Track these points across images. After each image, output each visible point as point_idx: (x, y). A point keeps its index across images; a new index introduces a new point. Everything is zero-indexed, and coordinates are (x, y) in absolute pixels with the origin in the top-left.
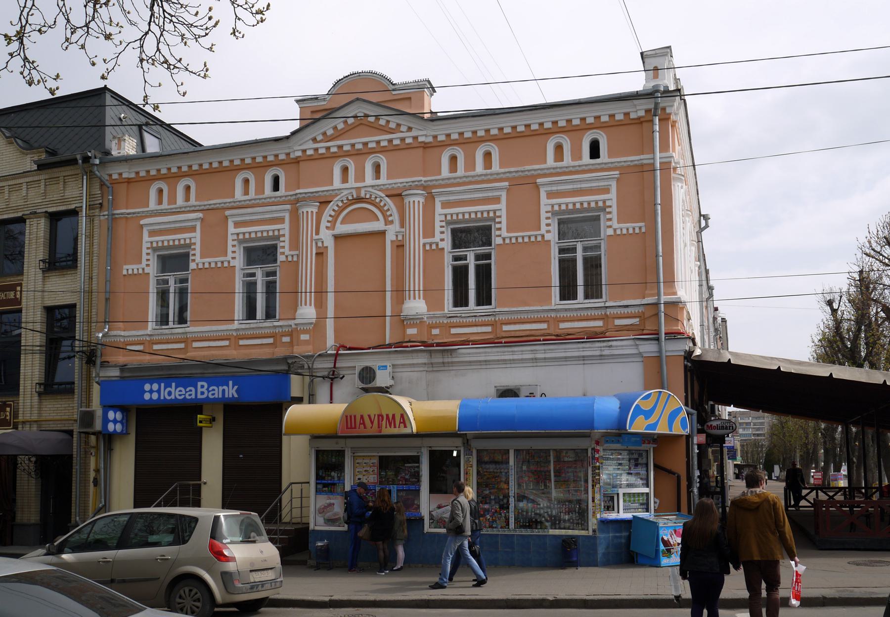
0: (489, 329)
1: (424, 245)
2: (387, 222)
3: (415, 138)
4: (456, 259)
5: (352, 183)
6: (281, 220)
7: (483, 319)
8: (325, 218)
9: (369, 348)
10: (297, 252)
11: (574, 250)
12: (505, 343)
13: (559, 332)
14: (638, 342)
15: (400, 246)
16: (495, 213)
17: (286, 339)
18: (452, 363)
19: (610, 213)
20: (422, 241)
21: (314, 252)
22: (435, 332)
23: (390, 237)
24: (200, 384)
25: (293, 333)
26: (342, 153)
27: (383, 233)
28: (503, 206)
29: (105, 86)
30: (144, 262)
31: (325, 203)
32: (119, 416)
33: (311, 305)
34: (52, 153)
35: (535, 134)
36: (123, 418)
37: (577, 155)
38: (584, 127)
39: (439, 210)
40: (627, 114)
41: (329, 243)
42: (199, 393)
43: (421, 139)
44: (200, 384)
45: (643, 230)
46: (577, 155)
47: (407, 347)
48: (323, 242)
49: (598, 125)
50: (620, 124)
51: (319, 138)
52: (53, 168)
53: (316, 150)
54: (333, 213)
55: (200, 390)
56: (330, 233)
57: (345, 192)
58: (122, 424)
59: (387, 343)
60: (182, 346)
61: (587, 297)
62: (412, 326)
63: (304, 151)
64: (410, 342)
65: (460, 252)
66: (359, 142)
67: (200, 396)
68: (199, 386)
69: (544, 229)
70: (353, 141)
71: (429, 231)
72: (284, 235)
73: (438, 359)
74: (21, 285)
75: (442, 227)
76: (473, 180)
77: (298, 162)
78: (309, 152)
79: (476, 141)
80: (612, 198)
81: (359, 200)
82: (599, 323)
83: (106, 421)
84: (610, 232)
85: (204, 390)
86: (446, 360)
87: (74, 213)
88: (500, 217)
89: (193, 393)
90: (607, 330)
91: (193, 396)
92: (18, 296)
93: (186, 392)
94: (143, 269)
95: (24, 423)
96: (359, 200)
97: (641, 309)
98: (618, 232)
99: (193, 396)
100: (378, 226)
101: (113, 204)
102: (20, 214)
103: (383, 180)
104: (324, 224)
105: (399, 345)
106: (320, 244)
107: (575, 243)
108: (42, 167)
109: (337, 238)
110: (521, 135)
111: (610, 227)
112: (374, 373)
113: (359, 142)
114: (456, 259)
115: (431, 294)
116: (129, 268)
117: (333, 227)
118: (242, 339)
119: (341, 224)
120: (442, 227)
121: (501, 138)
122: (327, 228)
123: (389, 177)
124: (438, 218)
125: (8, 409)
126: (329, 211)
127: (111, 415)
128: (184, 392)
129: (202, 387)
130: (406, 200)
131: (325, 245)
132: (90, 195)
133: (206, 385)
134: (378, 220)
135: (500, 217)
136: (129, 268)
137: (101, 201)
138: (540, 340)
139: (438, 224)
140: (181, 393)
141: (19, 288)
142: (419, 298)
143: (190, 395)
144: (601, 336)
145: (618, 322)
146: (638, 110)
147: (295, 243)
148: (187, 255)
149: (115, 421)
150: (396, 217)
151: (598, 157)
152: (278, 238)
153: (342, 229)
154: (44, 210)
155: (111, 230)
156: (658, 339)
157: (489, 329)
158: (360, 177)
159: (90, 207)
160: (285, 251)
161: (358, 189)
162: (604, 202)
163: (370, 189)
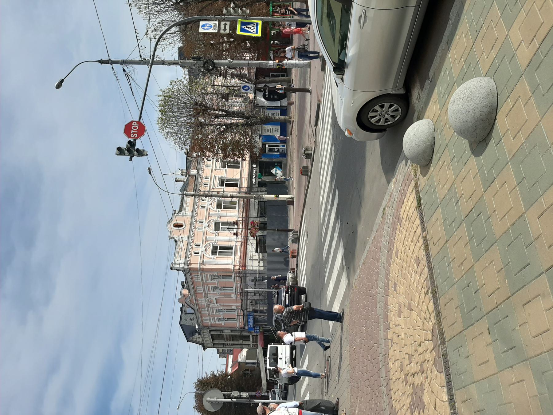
0: (238, 288)
2: (214, 298)
20: (218, 295)
27: (216, 299)
32: (256, 328)
39: (211, 292)
41: (218, 304)
60: (240, 319)
61: (223, 208)
69: (215, 281)
81: (208, 301)
109: (216, 303)
124: (213, 292)
127: (256, 331)
136: (223, 324)
139: (214, 292)
146: (188, 275)
148: (220, 318)
149: (257, 330)
152: (216, 309)
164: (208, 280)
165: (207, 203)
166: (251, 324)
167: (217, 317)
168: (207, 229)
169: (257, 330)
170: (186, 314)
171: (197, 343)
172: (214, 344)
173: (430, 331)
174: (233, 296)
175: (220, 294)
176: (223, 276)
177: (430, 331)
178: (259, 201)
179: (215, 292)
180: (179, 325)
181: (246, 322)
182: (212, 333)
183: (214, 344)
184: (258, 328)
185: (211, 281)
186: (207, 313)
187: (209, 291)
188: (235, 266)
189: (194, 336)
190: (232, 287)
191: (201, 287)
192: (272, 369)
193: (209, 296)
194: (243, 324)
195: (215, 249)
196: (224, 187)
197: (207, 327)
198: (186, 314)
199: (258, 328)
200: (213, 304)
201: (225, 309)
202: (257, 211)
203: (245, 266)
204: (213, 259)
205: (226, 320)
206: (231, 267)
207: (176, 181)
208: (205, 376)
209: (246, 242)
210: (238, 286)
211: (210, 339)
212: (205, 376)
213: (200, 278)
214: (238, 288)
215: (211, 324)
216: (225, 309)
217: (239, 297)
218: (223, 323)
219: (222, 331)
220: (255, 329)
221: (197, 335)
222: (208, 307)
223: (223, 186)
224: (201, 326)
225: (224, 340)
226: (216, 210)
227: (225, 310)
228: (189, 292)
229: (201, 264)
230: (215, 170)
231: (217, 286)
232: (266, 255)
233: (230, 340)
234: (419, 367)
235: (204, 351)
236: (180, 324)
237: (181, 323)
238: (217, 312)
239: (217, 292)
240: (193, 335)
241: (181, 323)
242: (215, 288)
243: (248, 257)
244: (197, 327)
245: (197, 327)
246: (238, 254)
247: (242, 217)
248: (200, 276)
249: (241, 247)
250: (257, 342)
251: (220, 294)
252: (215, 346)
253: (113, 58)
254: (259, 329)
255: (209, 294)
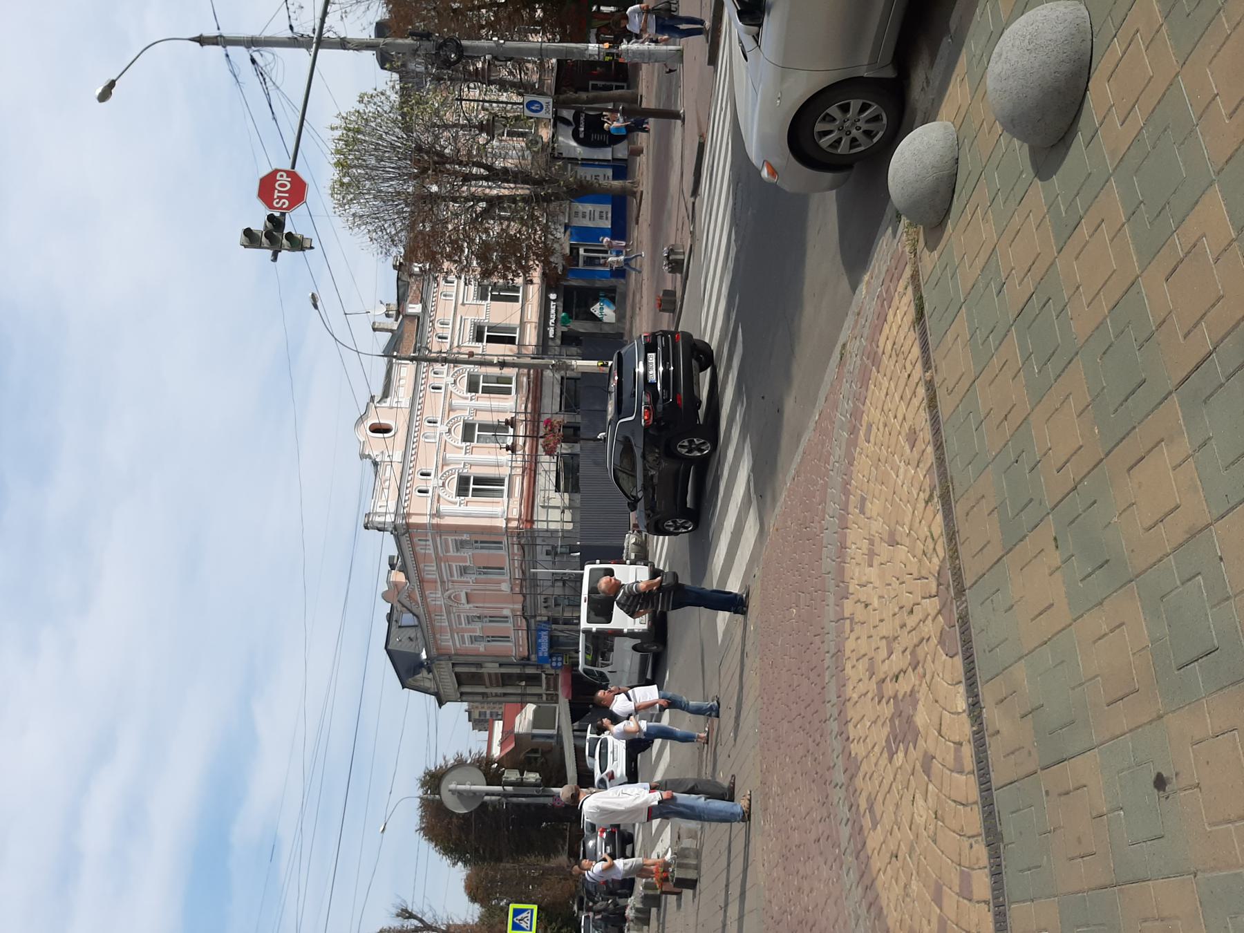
0: (517, 570)
23: (469, 591)
27: (467, 594)
32: (554, 659)
39: (455, 578)
41: (471, 605)
61: (482, 393)
81: (450, 597)
109: (468, 602)
124: (459, 579)
127: (554, 664)
136: (482, 649)
139: (462, 579)
146: (404, 539)
148: (475, 637)
149: (557, 661)
152: (468, 616)
153: (464, 600)
164: (447, 551)
165: (444, 381)
166: (544, 649)
167: (469, 634)
168: (445, 437)
169: (557, 661)
170: (400, 627)
171: (425, 691)
172: (462, 694)
173: (934, 576)
174: (505, 587)
175: (477, 581)
176: (482, 542)
177: (934, 576)
178: (562, 378)
179: (465, 579)
180: (385, 652)
181: (534, 645)
182: (458, 669)
183: (462, 694)
184: (560, 659)
185: (455, 554)
186: (447, 624)
187: (452, 575)
188: (508, 520)
189: (418, 677)
190: (503, 568)
191: (433, 566)
192: (594, 630)
193: (450, 587)
194: (526, 648)
195: (463, 483)
196: (485, 343)
197: (447, 657)
198: (400, 627)
199: (560, 659)
201: (486, 617)
202: (559, 399)
203: (532, 522)
204: (460, 504)
205: (489, 641)
206: (502, 523)
207: (375, 330)
208: (443, 764)
209: (533, 468)
210: (516, 565)
211: (453, 684)
212: (443, 764)
213: (432, 547)
214: (517, 570)
215: (456, 649)
216: (486, 617)
217: (517, 589)
218: (481, 647)
219: (480, 665)
220: (552, 661)
221: (424, 673)
222: (449, 613)
223: (487, 300)
224: (434, 652)
225: (484, 684)
226: (465, 395)
227: (488, 619)
228: (407, 578)
229: (432, 516)
230: (463, 304)
231: (468, 564)
232: (577, 497)
233: (498, 686)
234: (909, 657)
236: (386, 648)
237: (389, 647)
239: (469, 579)
240: (414, 674)
241: (389, 647)
242: (464, 571)
243: (539, 500)
244: (424, 656)
245: (424, 656)
246: (516, 495)
247: (526, 412)
248: (430, 543)
249: (523, 479)
250: (556, 689)
251: (477, 581)
252: (464, 698)
254: (562, 662)
255: (450, 584)
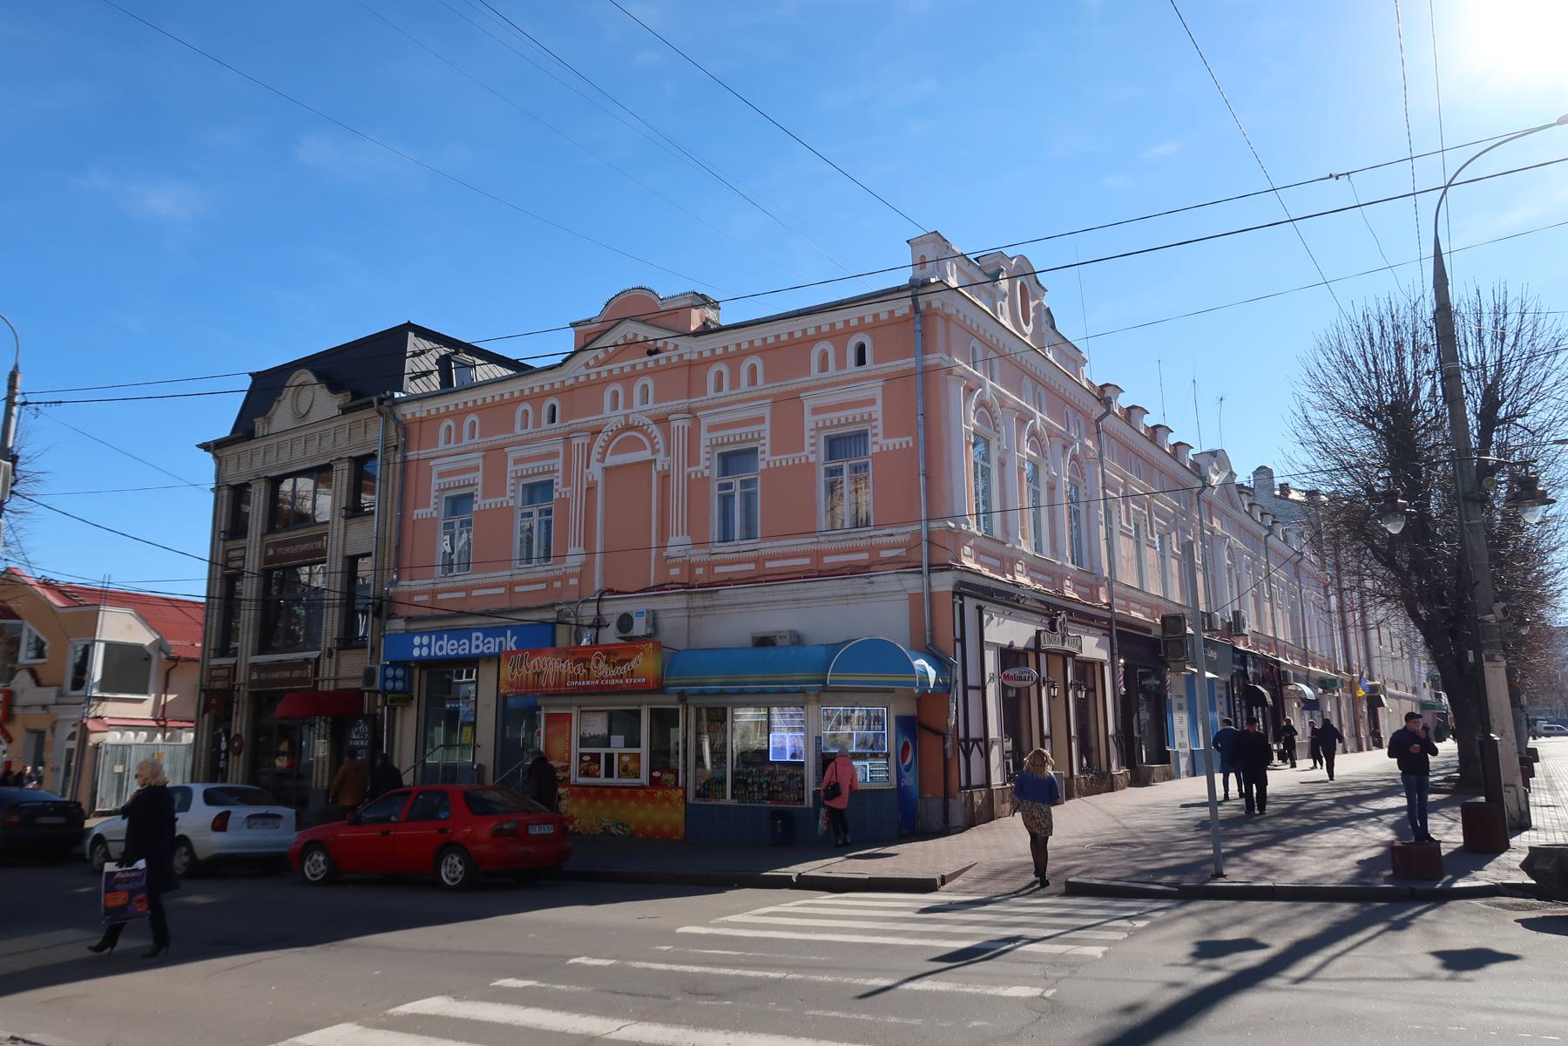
0: (752, 566)
1: (689, 475)
2: (655, 451)
3: (681, 356)
4: (722, 487)
5: (621, 411)
6: (554, 455)
7: (747, 554)
8: (596, 449)
9: (635, 593)
10: (569, 488)
11: (840, 471)
12: (766, 581)
13: (821, 568)
14: (901, 576)
15: (665, 477)
16: (759, 434)
17: (557, 584)
18: (713, 606)
19: (875, 427)
21: (585, 487)
22: (699, 571)
24: (474, 635)
25: (564, 578)
26: (612, 379)
28: (767, 426)
29: (409, 322)
30: (432, 506)
31: (596, 433)
32: (400, 673)
33: (579, 546)
34: (356, 395)
35: (800, 342)
36: (404, 675)
37: (841, 364)
38: (849, 331)
40: (891, 313)
42: (473, 647)
43: (686, 357)
44: (474, 635)
45: (911, 445)
46: (841, 364)
47: (667, 589)
48: (593, 476)
49: (862, 327)
50: (886, 324)
51: (592, 363)
52: (355, 411)
53: (588, 375)
54: (603, 444)
55: (474, 643)
56: (601, 465)
57: (616, 419)
58: (404, 682)
59: (652, 585)
60: (463, 594)
62: (674, 566)
63: (577, 378)
64: (672, 583)
65: (725, 480)
66: (626, 365)
67: (474, 651)
68: (474, 639)
70: (622, 365)
71: (693, 459)
72: (558, 471)
73: (698, 601)
74: (327, 534)
75: (707, 453)
76: (750, 396)
77: (572, 390)
78: (582, 379)
79: (741, 355)
80: (877, 411)
81: (628, 428)
82: (865, 556)
83: (385, 679)
84: (876, 449)
85: (479, 642)
86: (707, 603)
87: (373, 456)
88: (764, 438)
89: (467, 647)
90: (873, 564)
91: (467, 651)
92: (324, 546)
93: (459, 646)
94: (432, 513)
95: (323, 680)
96: (628, 428)
97: (908, 537)
98: (885, 449)
99: (467, 651)
100: (645, 455)
101: (406, 447)
102: (327, 461)
103: (650, 405)
104: (595, 456)
105: (660, 587)
106: (590, 479)
107: (841, 463)
108: (345, 410)
109: (606, 470)
110: (787, 345)
111: (877, 443)
112: (632, 619)
113: (626, 365)
114: (721, 487)
115: (694, 528)
116: (419, 513)
117: (602, 460)
118: (518, 585)
119: (611, 455)
120: (707, 453)
121: (764, 350)
122: (598, 460)
123: (655, 402)
125: (310, 666)
126: (600, 440)
127: (390, 672)
128: (456, 647)
129: (477, 638)
130: (674, 424)
131: (595, 479)
132: (386, 436)
133: (481, 635)
134: (645, 448)
135: (764, 438)
136: (419, 513)
137: (396, 444)
138: (800, 578)
140: (453, 647)
141: (325, 538)
142: (683, 534)
143: (463, 650)
144: (867, 570)
145: (885, 554)
147: (567, 482)
149: (394, 679)
150: (661, 446)
151: (864, 363)
153: (611, 460)
154: (348, 455)
155: (404, 473)
156: (921, 572)
157: (752, 566)
158: (629, 403)
159: (385, 449)
160: (559, 490)
161: (626, 417)
162: (870, 415)
163: (637, 415)
164: (816, 411)
166: (422, 647)
169: (394, 679)
179: (703, 456)
184: (399, 685)
200: (605, 449)
235: (206, 447)
236: (409, 327)
238: (523, 477)
239: (703, 463)
244: (397, 395)
253: (1360, 204)
